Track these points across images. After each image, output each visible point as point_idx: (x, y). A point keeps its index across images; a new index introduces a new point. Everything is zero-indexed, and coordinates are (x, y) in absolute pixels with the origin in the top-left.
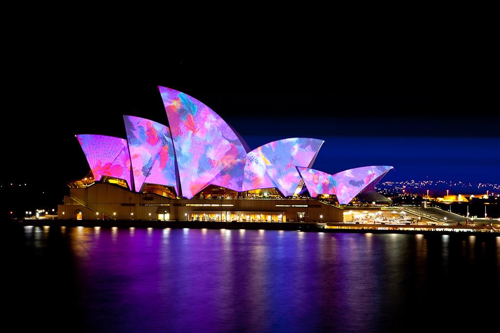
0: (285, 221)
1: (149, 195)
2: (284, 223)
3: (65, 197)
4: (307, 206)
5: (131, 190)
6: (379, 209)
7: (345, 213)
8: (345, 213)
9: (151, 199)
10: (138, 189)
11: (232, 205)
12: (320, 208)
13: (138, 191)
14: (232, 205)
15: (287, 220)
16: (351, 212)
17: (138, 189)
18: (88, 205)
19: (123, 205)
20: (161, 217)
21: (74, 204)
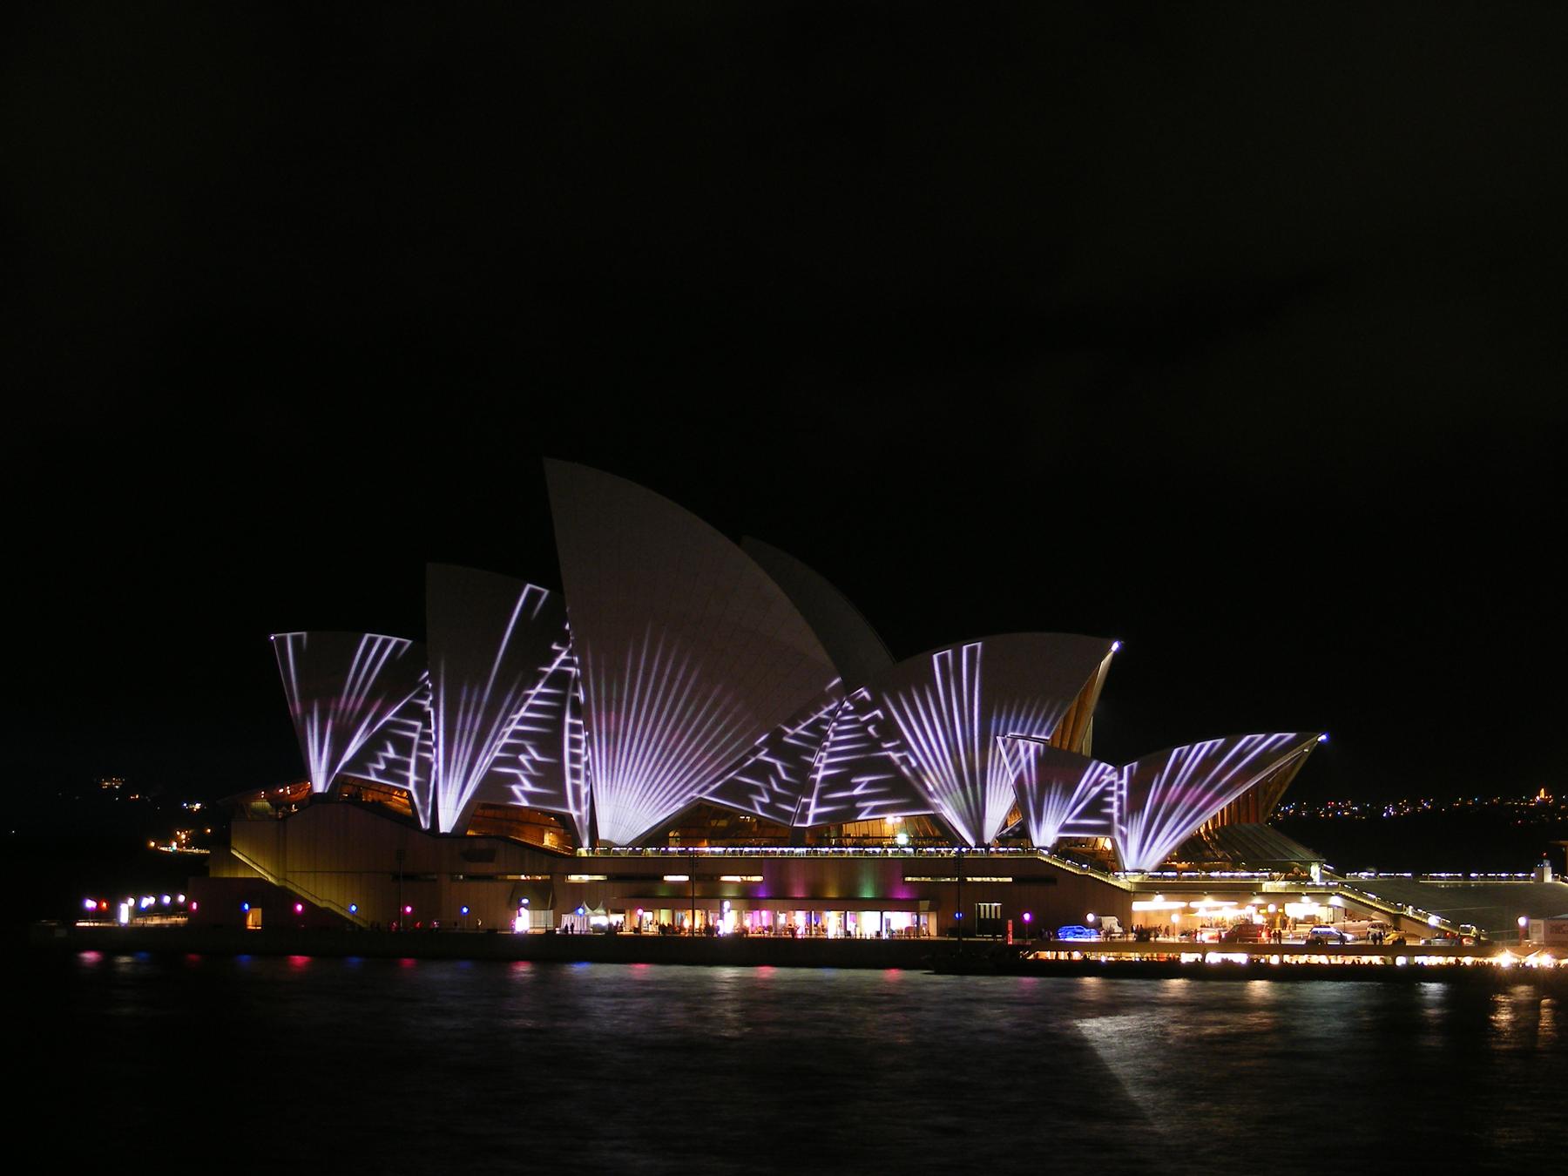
0: (933, 931)
2: (929, 944)
5: (425, 824)
7: (1138, 906)
8: (1138, 906)
9: (489, 856)
10: (447, 823)
11: (759, 879)
13: (449, 831)
14: (759, 879)
15: (940, 931)
16: (1158, 903)
17: (447, 823)
18: (289, 877)
19: (396, 877)
21: (241, 875)
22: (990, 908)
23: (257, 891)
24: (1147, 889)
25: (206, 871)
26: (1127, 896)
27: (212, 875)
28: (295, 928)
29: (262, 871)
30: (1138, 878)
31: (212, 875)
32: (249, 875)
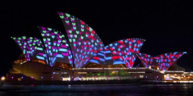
1: (58, 68)
3: (10, 70)
4: (145, 72)
6: (182, 73)
7: (165, 76)
8: (165, 76)
12: (152, 73)
19: (43, 73)
20: (64, 79)
21: (16, 73)
22: (141, 76)
23: (20, 75)
24: (166, 73)
25: (10, 73)
26: (163, 75)
27: (11, 73)
28: (27, 80)
29: (19, 72)
30: (164, 72)
31: (11, 73)
32: (18, 73)
